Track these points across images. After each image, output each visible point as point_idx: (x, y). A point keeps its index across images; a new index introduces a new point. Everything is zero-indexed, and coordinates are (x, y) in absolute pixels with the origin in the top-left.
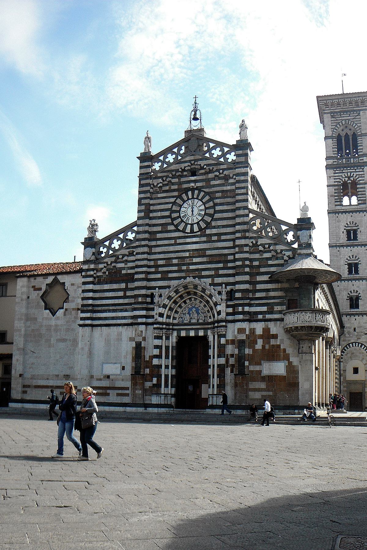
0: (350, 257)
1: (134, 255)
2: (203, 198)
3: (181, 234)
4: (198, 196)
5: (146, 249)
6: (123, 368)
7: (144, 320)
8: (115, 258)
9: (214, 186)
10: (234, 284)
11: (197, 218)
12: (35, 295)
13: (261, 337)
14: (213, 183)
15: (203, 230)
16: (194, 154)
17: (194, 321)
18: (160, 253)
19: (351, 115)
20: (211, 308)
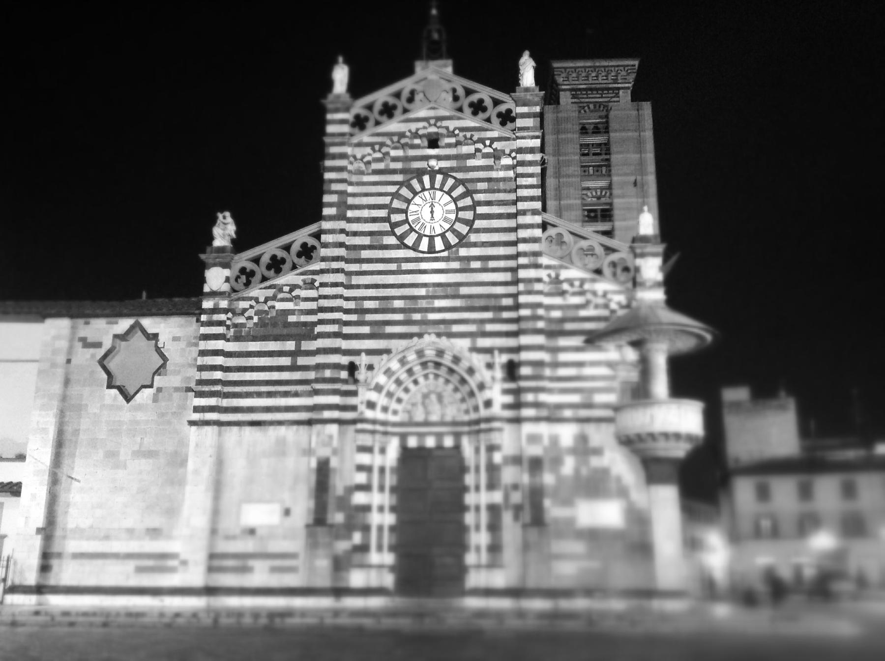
2: (453, 188)
3: (411, 254)
4: (443, 184)
5: (340, 278)
6: (287, 512)
7: (336, 414)
8: (275, 290)
10: (518, 349)
11: (441, 226)
12: (85, 358)
13: (574, 451)
14: (471, 163)
15: (454, 249)
16: (436, 106)
17: (434, 418)
18: (367, 287)
19: (604, 96)
20: (472, 394)
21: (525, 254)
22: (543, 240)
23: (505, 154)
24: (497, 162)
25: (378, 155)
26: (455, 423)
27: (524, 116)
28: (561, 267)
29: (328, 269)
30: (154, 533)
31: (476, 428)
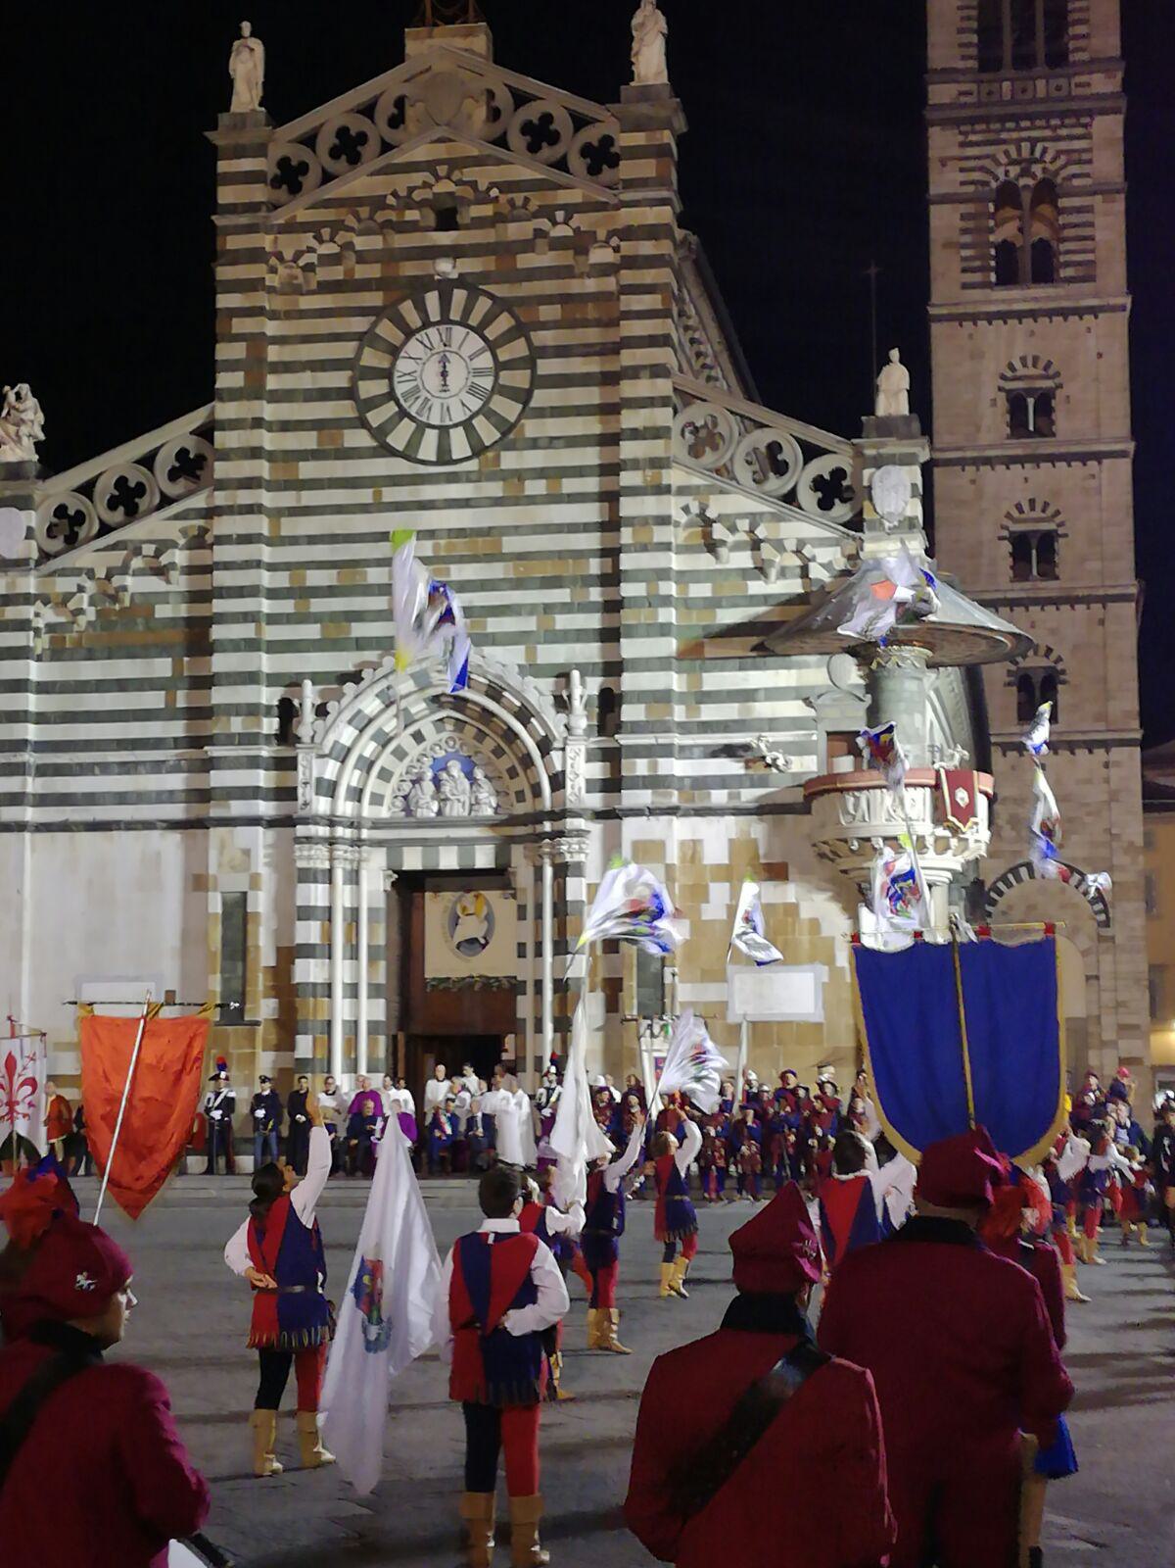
0: (1019, 508)
2: (488, 320)
3: (401, 467)
8: (125, 552)
9: (532, 274)
11: (463, 405)
14: (525, 261)
15: (490, 454)
16: (451, 137)
17: (456, 810)
18: (312, 540)
21: (635, 464)
23: (596, 241)
24: (581, 258)
27: (636, 153)
29: (232, 506)
31: (539, 828)
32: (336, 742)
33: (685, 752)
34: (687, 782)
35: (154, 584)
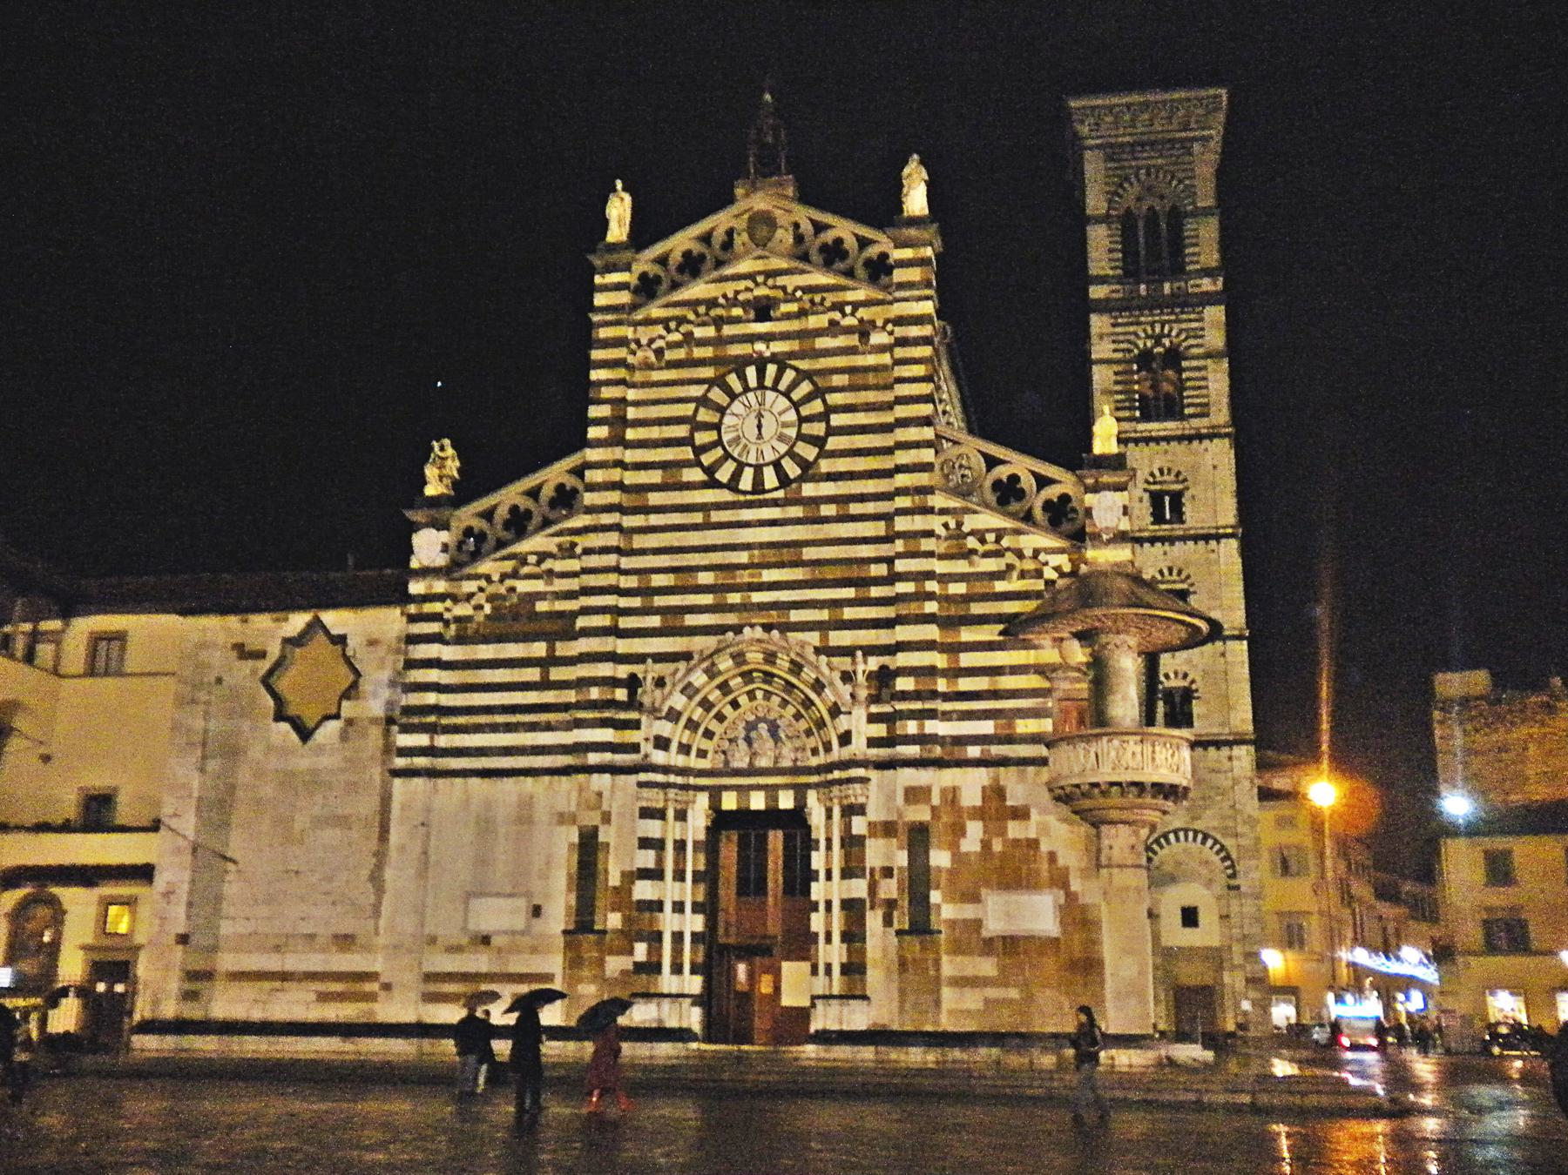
0: (1161, 572)
1: (573, 556)
2: (794, 385)
3: (725, 496)
4: (777, 380)
5: (613, 539)
7: (607, 757)
13: (979, 813)
14: (823, 343)
15: (794, 486)
17: (763, 762)
20: (821, 724)
22: (937, 467)
25: (676, 337)
26: (795, 771)
28: (967, 511)
30: (345, 941)
31: (830, 777)
32: (671, 708)
33: (946, 716)
34: (948, 740)
35: (538, 586)
